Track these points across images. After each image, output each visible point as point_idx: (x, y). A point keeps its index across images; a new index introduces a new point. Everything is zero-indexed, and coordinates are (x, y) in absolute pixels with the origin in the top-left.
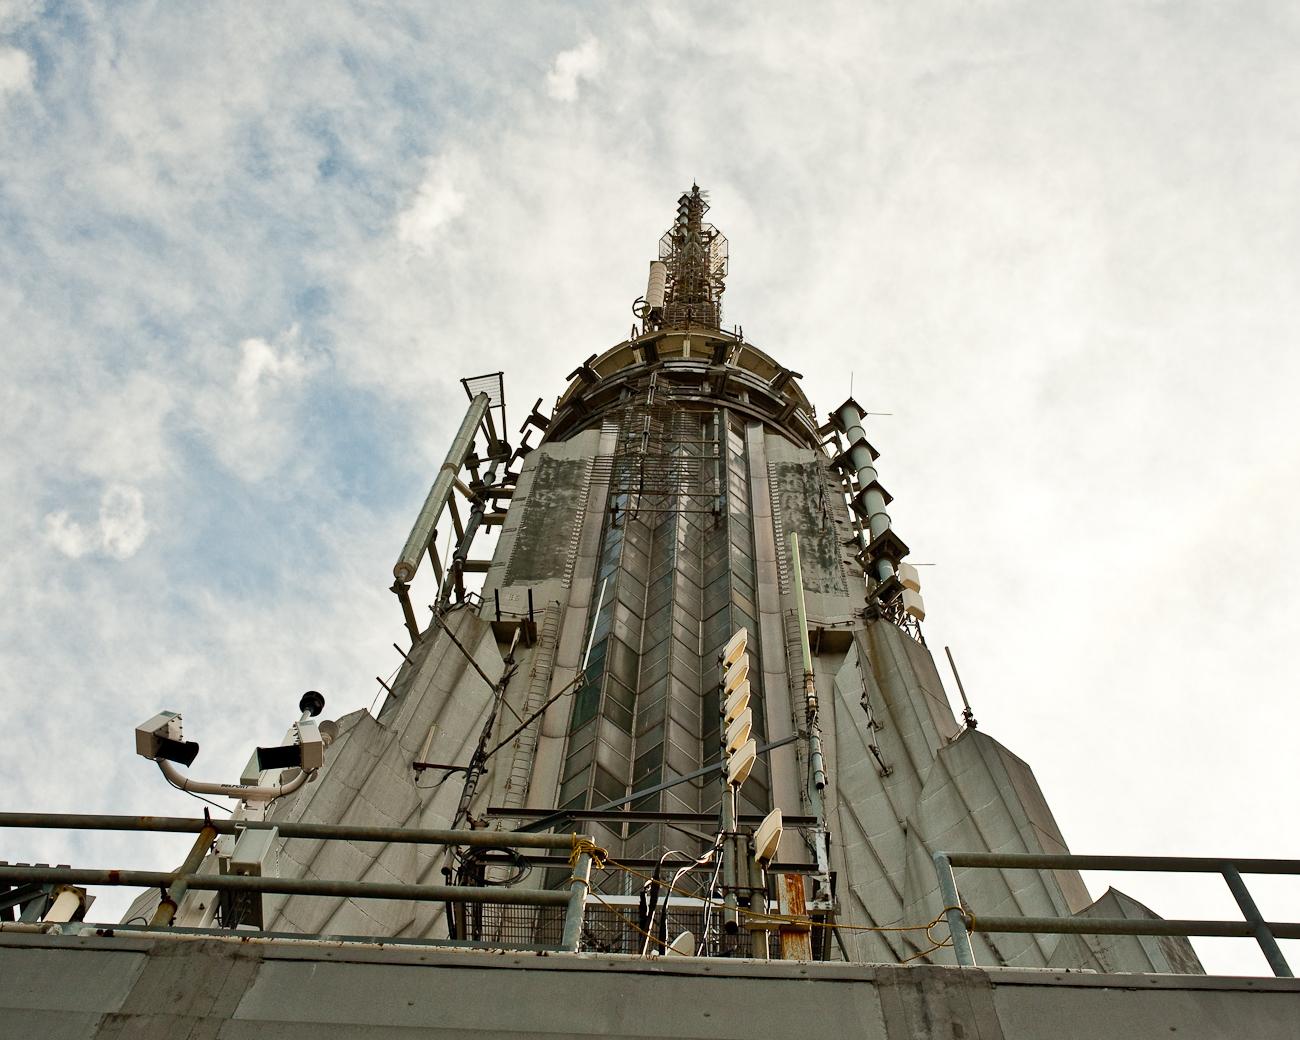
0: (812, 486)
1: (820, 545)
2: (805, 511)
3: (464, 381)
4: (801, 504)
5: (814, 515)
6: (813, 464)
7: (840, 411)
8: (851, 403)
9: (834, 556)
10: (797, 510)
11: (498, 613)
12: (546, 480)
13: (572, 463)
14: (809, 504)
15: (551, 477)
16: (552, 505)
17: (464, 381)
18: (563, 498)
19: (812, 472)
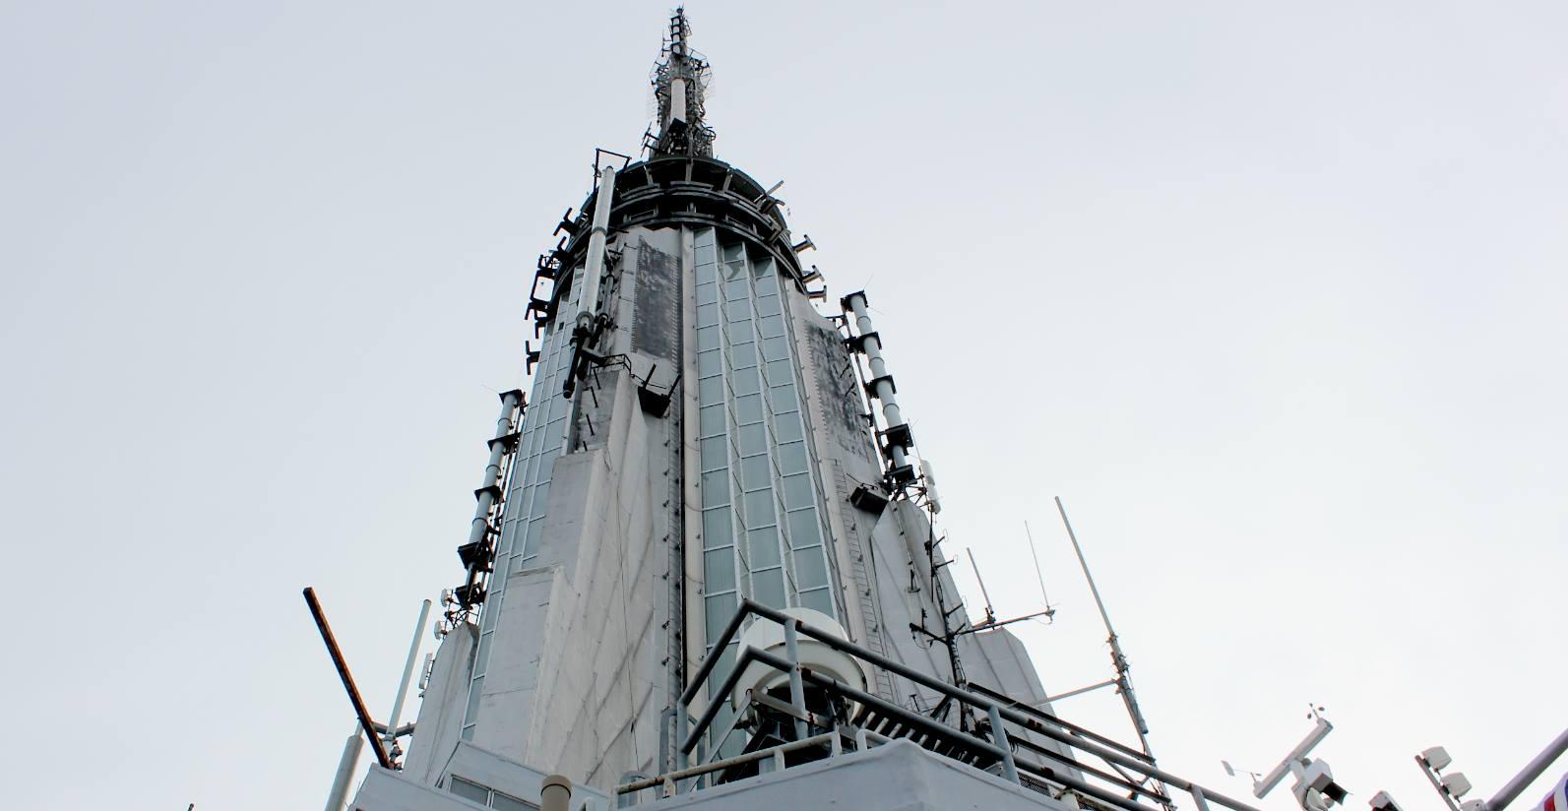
0: (832, 353)
1: (844, 408)
2: (830, 373)
3: (598, 150)
4: (827, 366)
5: (836, 379)
6: (831, 333)
7: (850, 297)
8: (861, 294)
9: (855, 423)
10: (825, 368)
11: (645, 383)
12: (646, 262)
13: (662, 254)
14: (832, 368)
15: (649, 261)
16: (653, 288)
17: (598, 150)
18: (659, 285)
19: (830, 339)
